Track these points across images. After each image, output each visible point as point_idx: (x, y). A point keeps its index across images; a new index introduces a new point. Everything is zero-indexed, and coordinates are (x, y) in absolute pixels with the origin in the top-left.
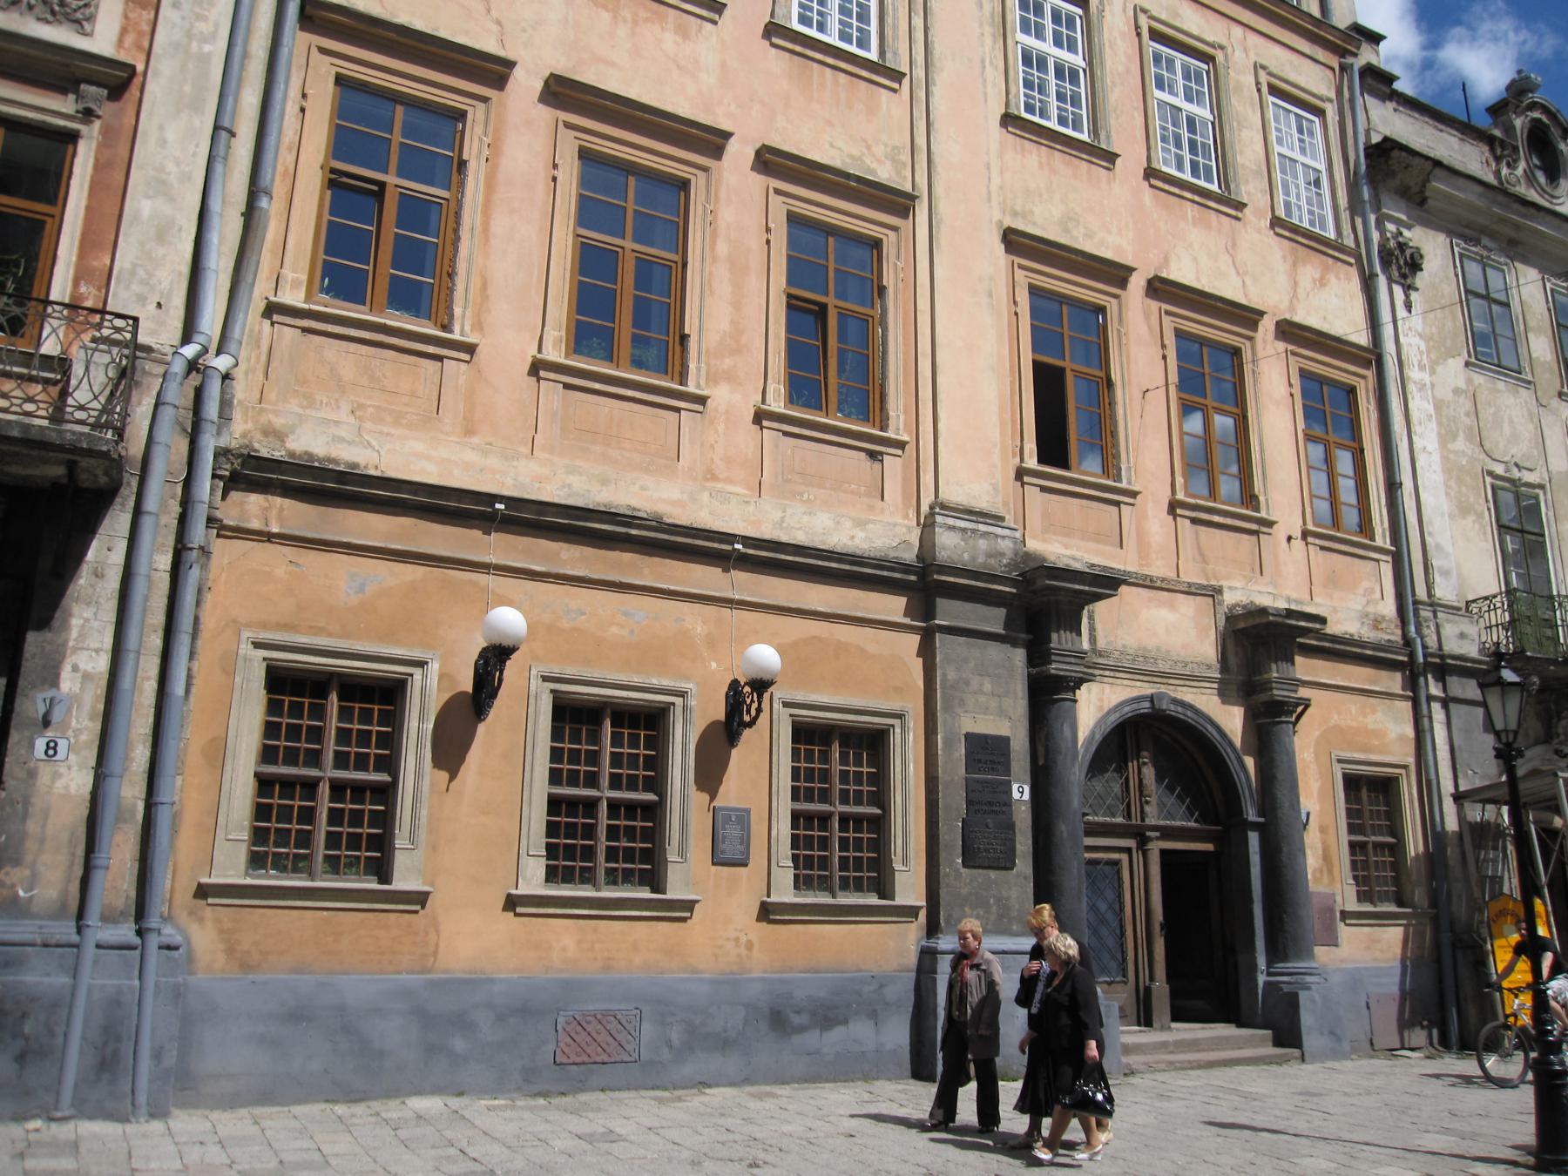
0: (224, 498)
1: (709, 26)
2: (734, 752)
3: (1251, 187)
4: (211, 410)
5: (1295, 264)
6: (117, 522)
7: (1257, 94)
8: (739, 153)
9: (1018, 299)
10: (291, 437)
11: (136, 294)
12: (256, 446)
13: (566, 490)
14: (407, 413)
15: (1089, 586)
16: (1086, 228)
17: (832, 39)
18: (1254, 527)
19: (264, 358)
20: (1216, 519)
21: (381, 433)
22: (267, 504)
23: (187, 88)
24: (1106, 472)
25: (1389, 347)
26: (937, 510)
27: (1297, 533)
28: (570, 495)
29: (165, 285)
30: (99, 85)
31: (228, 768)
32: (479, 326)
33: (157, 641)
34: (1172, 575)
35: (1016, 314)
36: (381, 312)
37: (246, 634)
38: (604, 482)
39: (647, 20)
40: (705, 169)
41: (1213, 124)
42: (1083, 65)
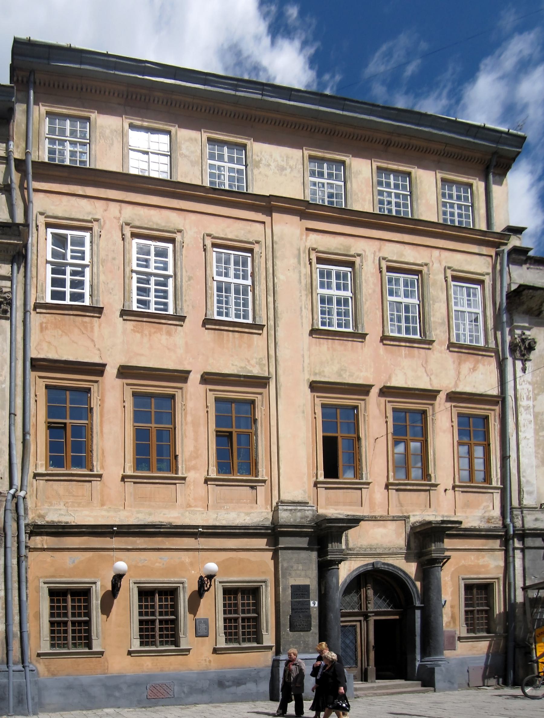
0: (29, 539)
2: (202, 600)
4: (22, 512)
8: (194, 378)
9: (316, 411)
10: (47, 517)
12: (37, 521)
15: (346, 524)
17: (232, 319)
21: (74, 510)
24: (355, 477)
26: (280, 504)
28: (138, 521)
31: (41, 620)
32: (102, 467)
33: (16, 585)
34: (386, 514)
35: (315, 418)
36: (70, 470)
37: (41, 580)
40: (181, 388)
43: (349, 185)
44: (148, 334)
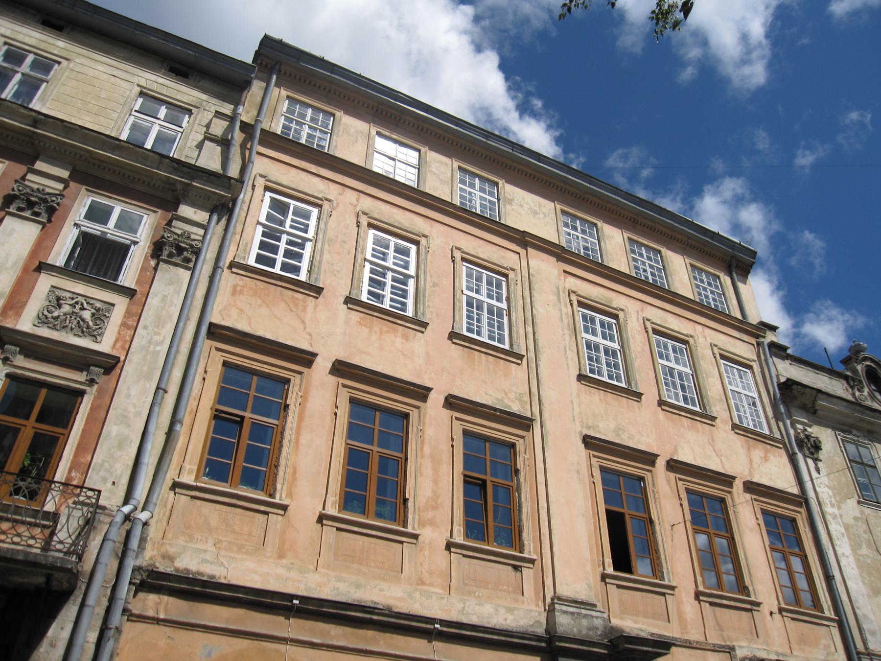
0: (134, 596)
1: (420, 334)
3: (718, 408)
4: (134, 543)
5: (749, 449)
6: (69, 612)
7: (714, 360)
8: (436, 399)
9: (594, 474)
10: (178, 560)
11: (102, 477)
12: (157, 565)
13: (335, 591)
14: (245, 545)
15: (652, 647)
16: (629, 434)
17: (485, 339)
18: (748, 606)
19: (168, 513)
20: (725, 602)
21: (230, 557)
22: (159, 601)
23: (145, 368)
24: (655, 575)
25: (811, 494)
26: (556, 601)
27: (775, 610)
28: (338, 595)
29: (119, 472)
30: (99, 367)
32: (290, 495)
35: (594, 483)
36: (236, 487)
38: (358, 586)
39: (387, 332)
40: (418, 407)
41: (692, 375)
42: (619, 348)
43: (602, 244)
44: (378, 331)
